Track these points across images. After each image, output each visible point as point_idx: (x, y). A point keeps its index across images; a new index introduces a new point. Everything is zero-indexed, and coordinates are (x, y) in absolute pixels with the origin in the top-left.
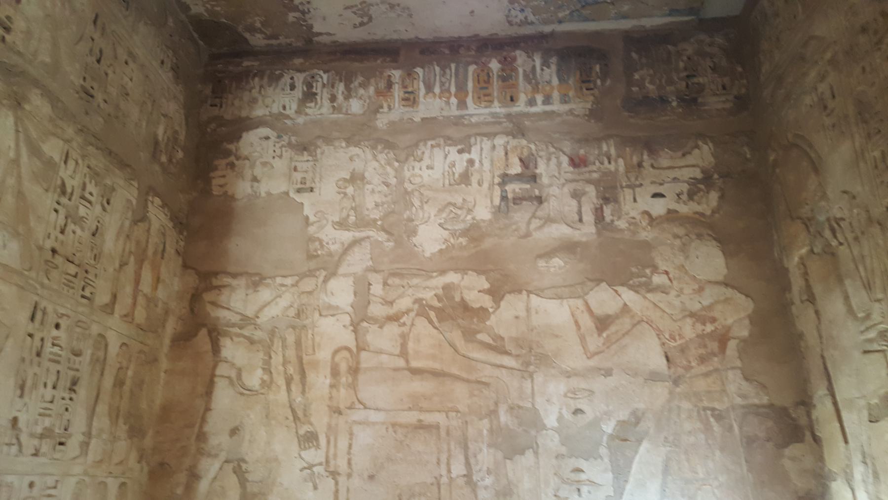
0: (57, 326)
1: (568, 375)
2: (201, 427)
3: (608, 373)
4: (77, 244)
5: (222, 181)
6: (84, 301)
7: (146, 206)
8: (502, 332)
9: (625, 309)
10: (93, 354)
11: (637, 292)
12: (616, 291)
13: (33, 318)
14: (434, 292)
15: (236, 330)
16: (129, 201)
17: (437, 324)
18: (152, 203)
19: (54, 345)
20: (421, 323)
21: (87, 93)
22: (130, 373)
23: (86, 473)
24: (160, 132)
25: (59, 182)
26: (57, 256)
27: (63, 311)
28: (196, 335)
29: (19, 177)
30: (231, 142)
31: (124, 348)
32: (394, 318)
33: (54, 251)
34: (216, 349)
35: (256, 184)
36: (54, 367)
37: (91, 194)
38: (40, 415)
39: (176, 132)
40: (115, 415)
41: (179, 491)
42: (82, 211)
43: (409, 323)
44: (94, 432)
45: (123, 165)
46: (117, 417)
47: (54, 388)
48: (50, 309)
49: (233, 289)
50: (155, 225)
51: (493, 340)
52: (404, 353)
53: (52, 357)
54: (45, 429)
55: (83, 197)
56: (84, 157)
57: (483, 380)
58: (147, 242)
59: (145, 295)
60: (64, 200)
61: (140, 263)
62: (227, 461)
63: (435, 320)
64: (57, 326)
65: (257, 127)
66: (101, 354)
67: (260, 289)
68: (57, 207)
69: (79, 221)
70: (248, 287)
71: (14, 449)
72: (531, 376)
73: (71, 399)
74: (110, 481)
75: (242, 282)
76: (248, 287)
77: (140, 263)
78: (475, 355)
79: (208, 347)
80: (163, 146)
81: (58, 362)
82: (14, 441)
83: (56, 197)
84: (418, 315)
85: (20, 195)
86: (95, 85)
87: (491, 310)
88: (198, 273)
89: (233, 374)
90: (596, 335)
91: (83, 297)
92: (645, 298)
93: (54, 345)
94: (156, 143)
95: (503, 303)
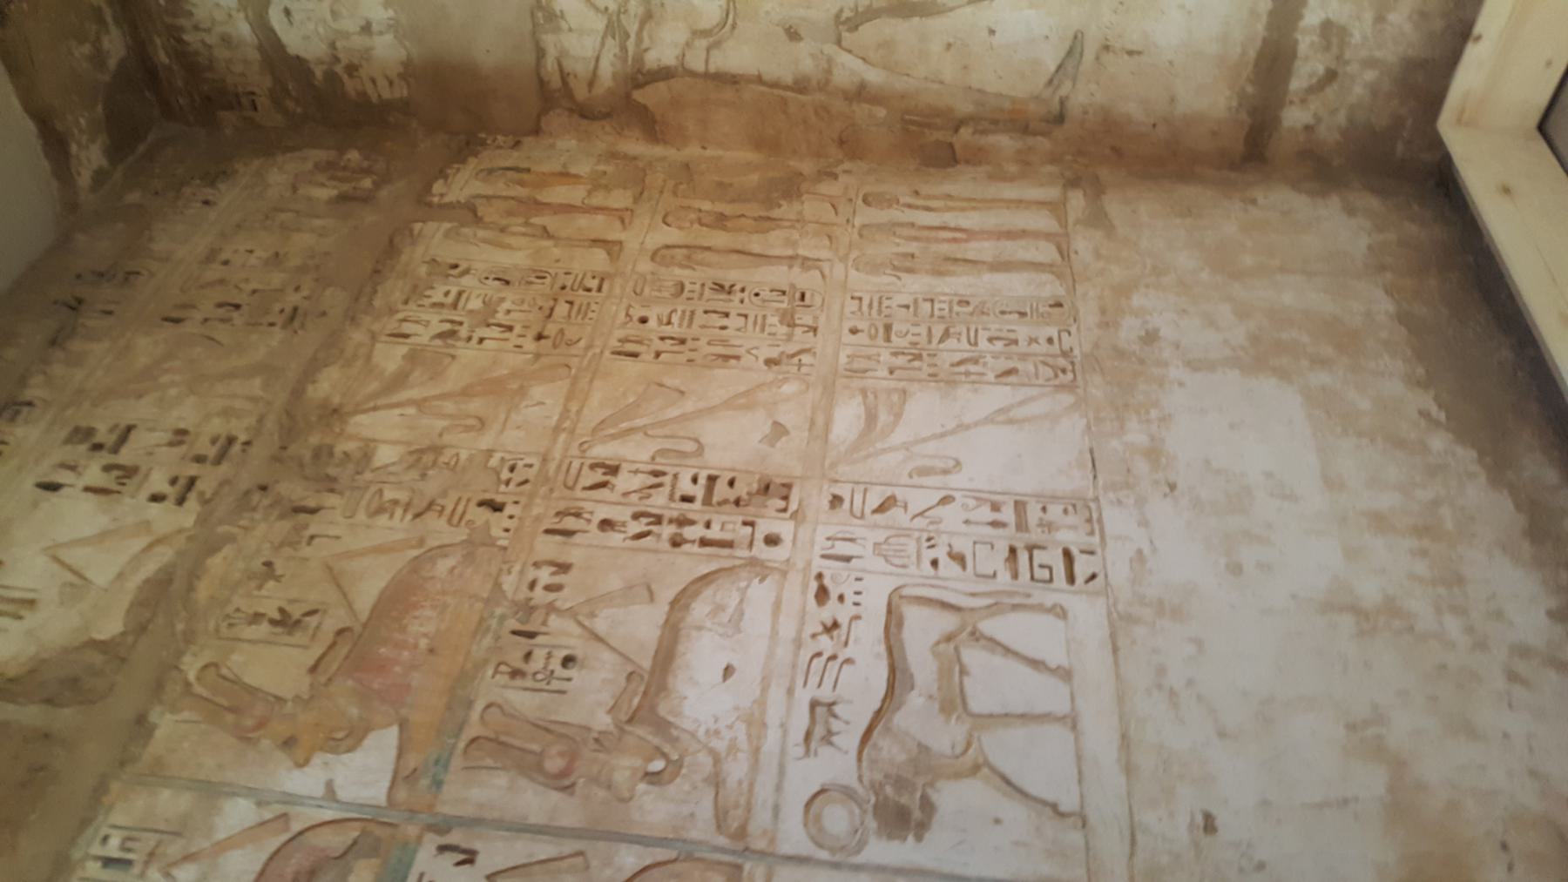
0: (644, 320)
2: (787, 88)
4: (525, 307)
5: (382, 83)
6: (605, 286)
7: (451, 206)
10: (682, 266)
13: (635, 355)
15: (631, 44)
16: (447, 235)
18: (442, 195)
19: (669, 323)
21: (292, 318)
22: (706, 206)
23: (844, 259)
24: (324, 193)
25: (438, 342)
26: (546, 333)
27: (622, 315)
28: (645, 107)
29: (444, 396)
30: (311, 73)
31: (670, 219)
33: (540, 337)
34: (665, 74)
35: (375, 27)
36: (700, 318)
37: (447, 294)
38: (763, 330)
39: (317, 166)
40: (766, 223)
41: (881, 112)
42: (475, 304)
44: (790, 252)
45: (392, 249)
46: (769, 218)
47: (727, 315)
48: (620, 333)
50: (478, 187)
53: (685, 323)
54: (781, 322)
55: (455, 306)
56: (392, 311)
58: (506, 198)
59: (589, 193)
60: (463, 332)
61: (540, 206)
62: (839, 42)
64: (644, 320)
65: (272, 31)
66: (679, 253)
67: (557, 9)
69: (490, 306)
70: (557, 30)
71: (806, 359)
73: (743, 290)
74: (858, 221)
75: (549, 40)
76: (557, 30)
77: (540, 206)
79: (662, 85)
80: (346, 187)
81: (693, 313)
82: (796, 360)
83: (459, 344)
85: (466, 393)
86: (277, 307)
88: (544, 111)
89: (702, 43)
91: (599, 289)
93: (669, 323)
94: (343, 198)
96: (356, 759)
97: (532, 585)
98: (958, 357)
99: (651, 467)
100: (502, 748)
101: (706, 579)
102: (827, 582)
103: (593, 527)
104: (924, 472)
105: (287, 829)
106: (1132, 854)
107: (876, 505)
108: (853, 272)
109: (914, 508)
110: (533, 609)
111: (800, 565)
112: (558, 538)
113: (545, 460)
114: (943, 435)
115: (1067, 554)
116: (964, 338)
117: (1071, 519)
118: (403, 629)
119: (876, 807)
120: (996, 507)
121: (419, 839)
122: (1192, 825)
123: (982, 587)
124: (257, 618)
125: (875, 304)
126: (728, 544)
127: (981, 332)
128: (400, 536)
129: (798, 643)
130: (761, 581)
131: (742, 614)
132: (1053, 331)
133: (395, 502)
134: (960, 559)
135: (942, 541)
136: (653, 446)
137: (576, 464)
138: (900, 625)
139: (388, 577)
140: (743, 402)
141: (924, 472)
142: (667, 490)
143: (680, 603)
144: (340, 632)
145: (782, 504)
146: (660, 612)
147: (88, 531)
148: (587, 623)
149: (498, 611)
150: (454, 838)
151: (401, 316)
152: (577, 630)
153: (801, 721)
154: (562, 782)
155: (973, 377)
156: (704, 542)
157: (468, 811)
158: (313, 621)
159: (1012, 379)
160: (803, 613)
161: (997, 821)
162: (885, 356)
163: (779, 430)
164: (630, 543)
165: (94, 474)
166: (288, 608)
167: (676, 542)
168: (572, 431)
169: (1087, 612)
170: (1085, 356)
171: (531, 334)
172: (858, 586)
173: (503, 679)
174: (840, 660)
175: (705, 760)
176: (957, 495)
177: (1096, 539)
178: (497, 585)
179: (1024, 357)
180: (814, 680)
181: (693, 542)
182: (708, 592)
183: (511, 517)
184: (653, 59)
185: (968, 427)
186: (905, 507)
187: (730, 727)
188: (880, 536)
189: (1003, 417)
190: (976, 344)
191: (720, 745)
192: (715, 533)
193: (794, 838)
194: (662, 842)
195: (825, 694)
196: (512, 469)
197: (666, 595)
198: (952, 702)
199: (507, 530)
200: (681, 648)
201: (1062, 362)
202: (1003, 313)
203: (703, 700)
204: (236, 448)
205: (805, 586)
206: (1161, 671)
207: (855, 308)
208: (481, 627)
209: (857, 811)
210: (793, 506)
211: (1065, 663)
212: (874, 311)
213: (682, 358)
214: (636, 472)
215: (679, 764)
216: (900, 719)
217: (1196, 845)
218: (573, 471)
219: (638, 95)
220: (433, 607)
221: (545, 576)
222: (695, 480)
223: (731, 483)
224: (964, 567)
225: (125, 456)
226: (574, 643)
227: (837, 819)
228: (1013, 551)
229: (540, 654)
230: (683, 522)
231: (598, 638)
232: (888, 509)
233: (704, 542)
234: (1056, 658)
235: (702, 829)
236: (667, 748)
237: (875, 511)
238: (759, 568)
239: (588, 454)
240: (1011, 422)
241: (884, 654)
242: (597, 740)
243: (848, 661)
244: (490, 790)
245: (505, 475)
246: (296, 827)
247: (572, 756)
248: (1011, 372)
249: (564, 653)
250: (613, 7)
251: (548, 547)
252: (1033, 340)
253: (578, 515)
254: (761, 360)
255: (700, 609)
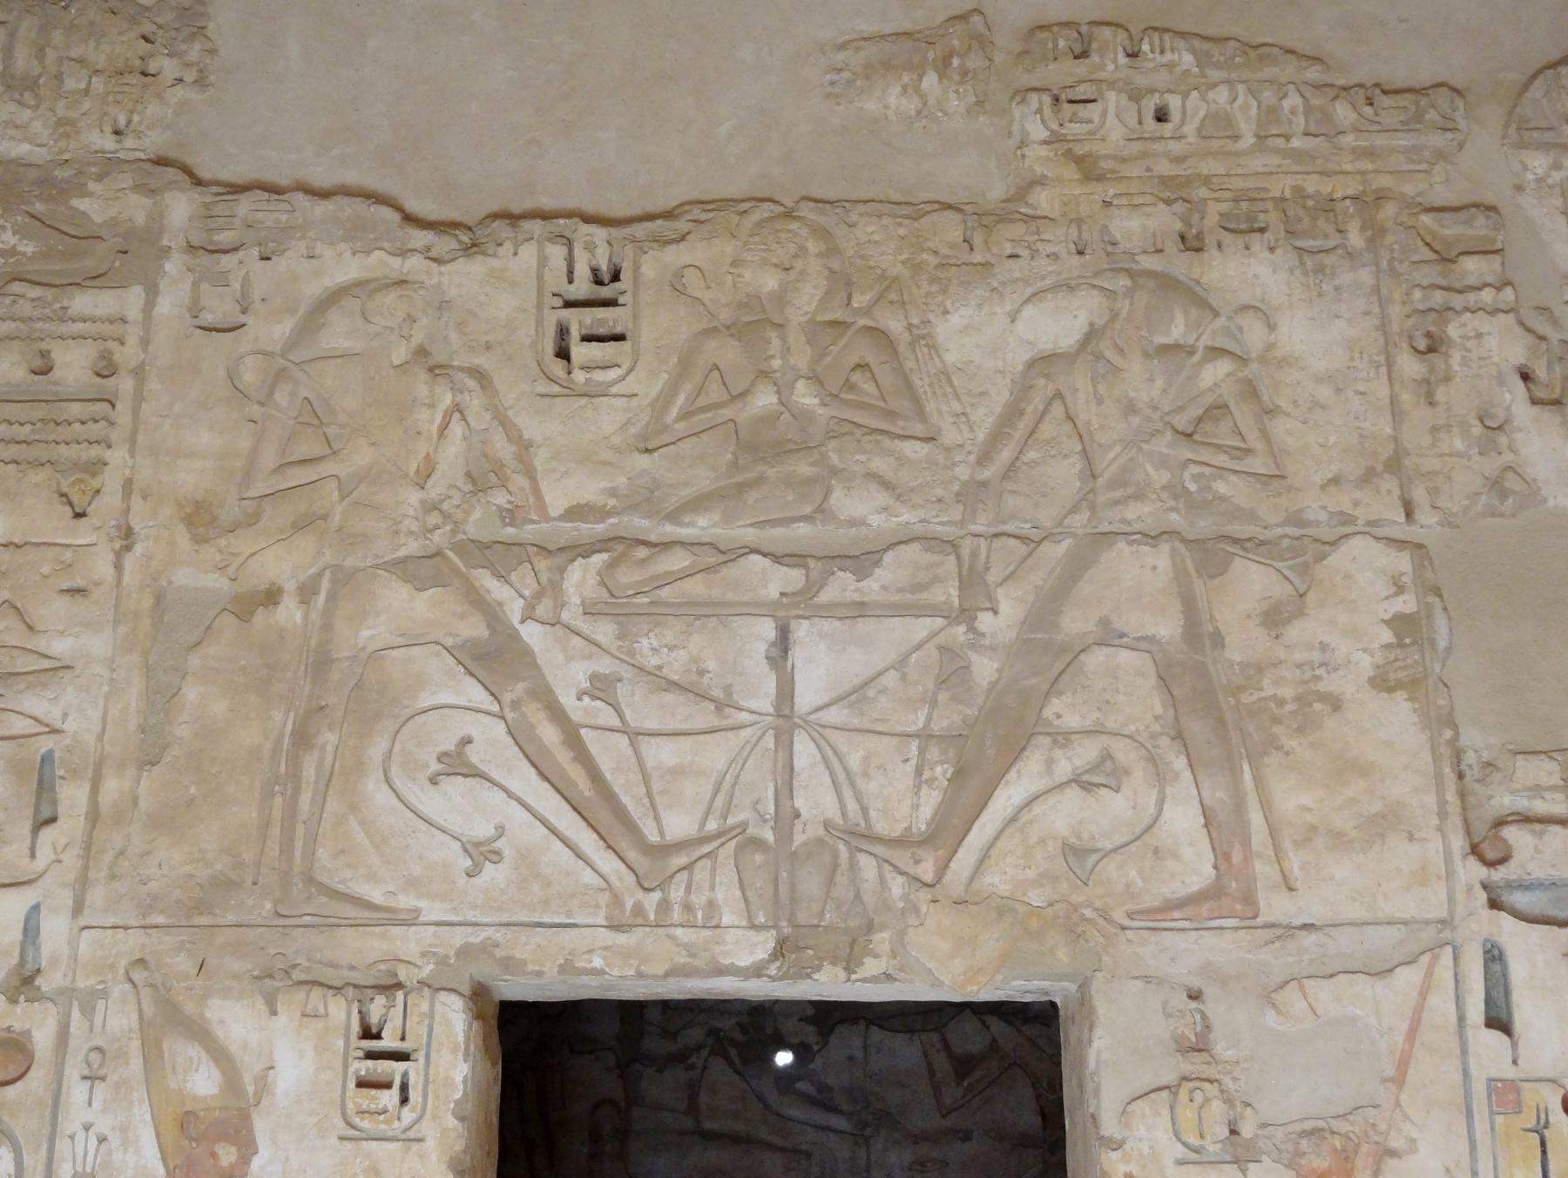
1: (916, 1139)
3: (966, 1137)
8: (832, 1081)
9: (994, 1046)
11: (1010, 1023)
12: (984, 1023)
14: (734, 1021)
17: (739, 1067)
20: (718, 1068)
32: (680, 1058)
43: (700, 1064)
51: (820, 1091)
52: (692, 1108)
57: (804, 1147)
63: (737, 1061)
72: (867, 1143)
78: (794, 1113)
84: (712, 1053)
87: (816, 1048)
90: (953, 1084)
92: (1019, 1031)
95: (833, 1040)
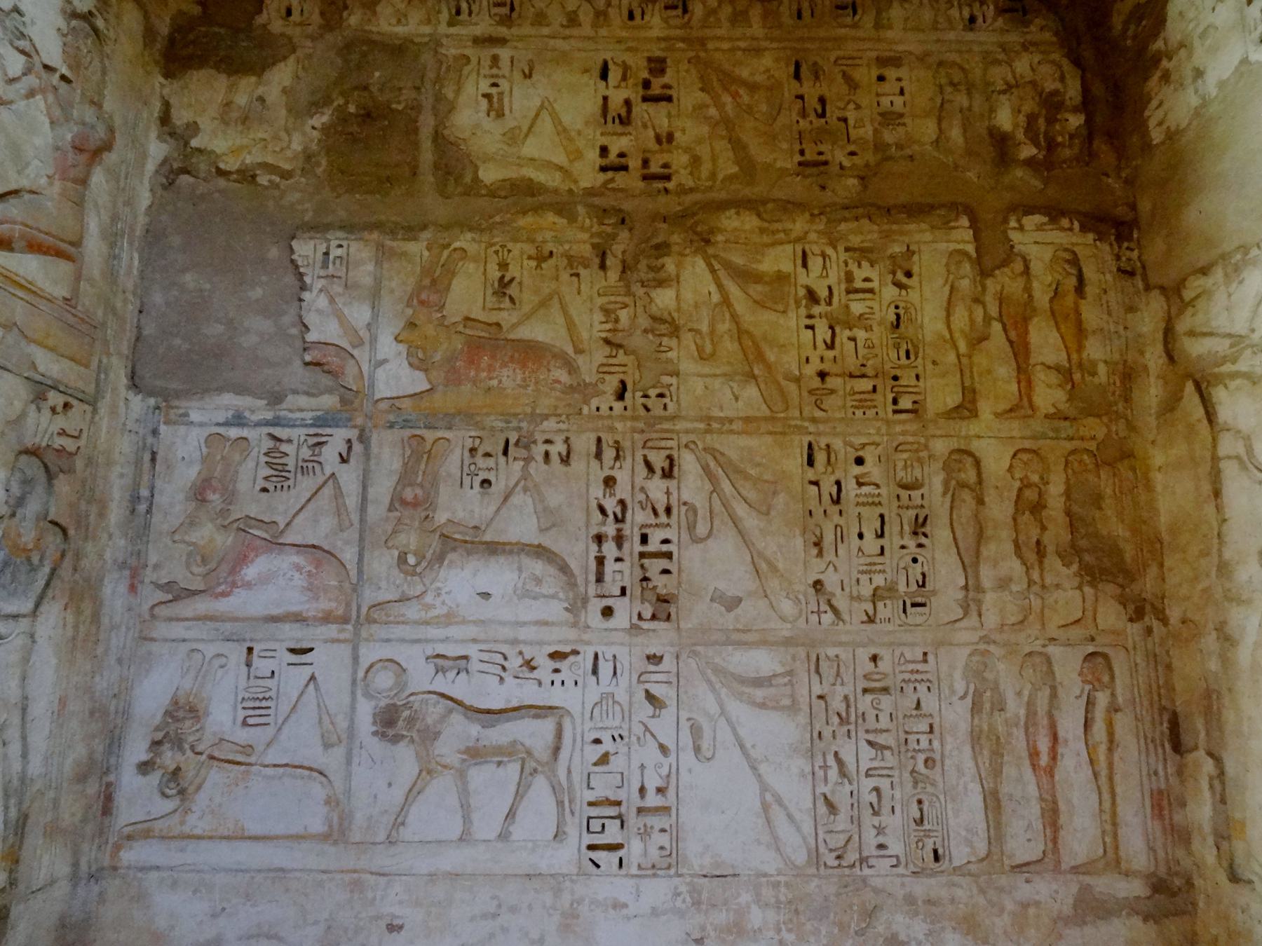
0: (860, 461)
5: (1159, 114)
10: (946, 484)
13: (811, 462)
19: (860, 484)
26: (828, 379)
27: (864, 440)
29: (735, 318)
38: (863, 572)
41: (1213, 665)
42: (857, 308)
48: (837, 444)
49: (1205, 293)
60: (816, 310)
64: (860, 461)
67: (1245, 274)
68: (809, 322)
71: (828, 618)
75: (1218, 273)
79: (1200, 412)
82: (824, 607)
85: (741, 333)
93: (860, 484)
96: (405, 370)
97: (548, 442)
98: (849, 758)
99: (674, 503)
100: (420, 456)
101: (564, 569)
102: (572, 658)
103: (607, 472)
104: (696, 731)
105: (354, 347)
106: (372, 873)
107: (652, 691)
108: (967, 651)
109: (652, 724)
110: (527, 447)
111: (585, 637)
112: (593, 449)
113: (673, 418)
114: (742, 747)
115: (618, 847)
116: (875, 764)
117: (654, 853)
118: (504, 365)
119: (394, 705)
120: (660, 790)
121: (355, 427)
122: (394, 916)
123: (577, 777)
124: (503, 266)
125: (919, 677)
126: (600, 579)
127: (888, 781)
128: (585, 335)
129: (514, 642)
130: (566, 609)
131: (535, 598)
132: (896, 848)
133: (617, 321)
134: (604, 759)
135: (621, 747)
136: (700, 502)
137: (669, 443)
138: (536, 716)
139: (548, 341)
140: (761, 567)
141: (696, 731)
142: (652, 520)
143: (540, 551)
144: (498, 325)
145: (647, 614)
146: (533, 537)
147: (566, 119)
148: (518, 488)
149: (524, 425)
150: (357, 447)
151: (829, 251)
152: (512, 483)
153: (452, 650)
154: (398, 501)
155: (820, 773)
156: (600, 561)
157: (375, 449)
158: (506, 303)
159: (822, 809)
160: (541, 643)
161: (390, 785)
162: (840, 691)
163: (733, 603)
164: (594, 504)
165: (617, 98)
166: (514, 284)
167: (599, 539)
168: (708, 431)
169: (567, 856)
170: (864, 880)
171: (826, 367)
172: (569, 683)
173: (469, 443)
174: (503, 674)
175: (419, 589)
176: (672, 758)
177: (634, 871)
178: (546, 417)
179: (856, 821)
180: (485, 657)
181: (600, 551)
182: (552, 570)
183: (611, 409)
184: (1220, 395)
185: (754, 768)
186: (653, 717)
187: (443, 603)
188: (622, 696)
189: (769, 803)
190: (867, 775)
191: (429, 599)
192: (610, 566)
193: (369, 654)
194: (360, 572)
195: (475, 666)
196: (661, 395)
197: (546, 541)
198: (475, 754)
199: (598, 409)
200: (502, 559)
201: (852, 856)
202: (920, 802)
203: (460, 582)
204: (659, 185)
205: (566, 642)
206: (513, 910)
207: (909, 656)
208: (507, 416)
209: (393, 693)
210: (645, 625)
211: (514, 837)
212: (907, 676)
213: (813, 504)
214: (668, 493)
215: (414, 574)
216: (457, 718)
217: (378, 917)
218: (663, 444)
219: (1190, 387)
220: (524, 380)
221: (558, 448)
222: (666, 541)
223: (666, 571)
224: (595, 764)
225: (640, 109)
226: (498, 487)
227: (384, 680)
228: (619, 803)
229: (491, 462)
230: (619, 540)
231: (506, 499)
232: (651, 703)
233: (600, 561)
234: (517, 832)
235: (370, 596)
236: (424, 564)
237: (647, 691)
238: (577, 606)
239: (683, 450)
240: (765, 807)
241: (510, 706)
242: (427, 517)
243: (502, 678)
244: (388, 455)
245: (653, 393)
246: (355, 352)
247: (415, 504)
248: (832, 807)
249: (493, 479)
250: (1255, 337)
251: (584, 443)
252: (880, 830)
253: (617, 458)
254: (821, 577)
255: (538, 567)
